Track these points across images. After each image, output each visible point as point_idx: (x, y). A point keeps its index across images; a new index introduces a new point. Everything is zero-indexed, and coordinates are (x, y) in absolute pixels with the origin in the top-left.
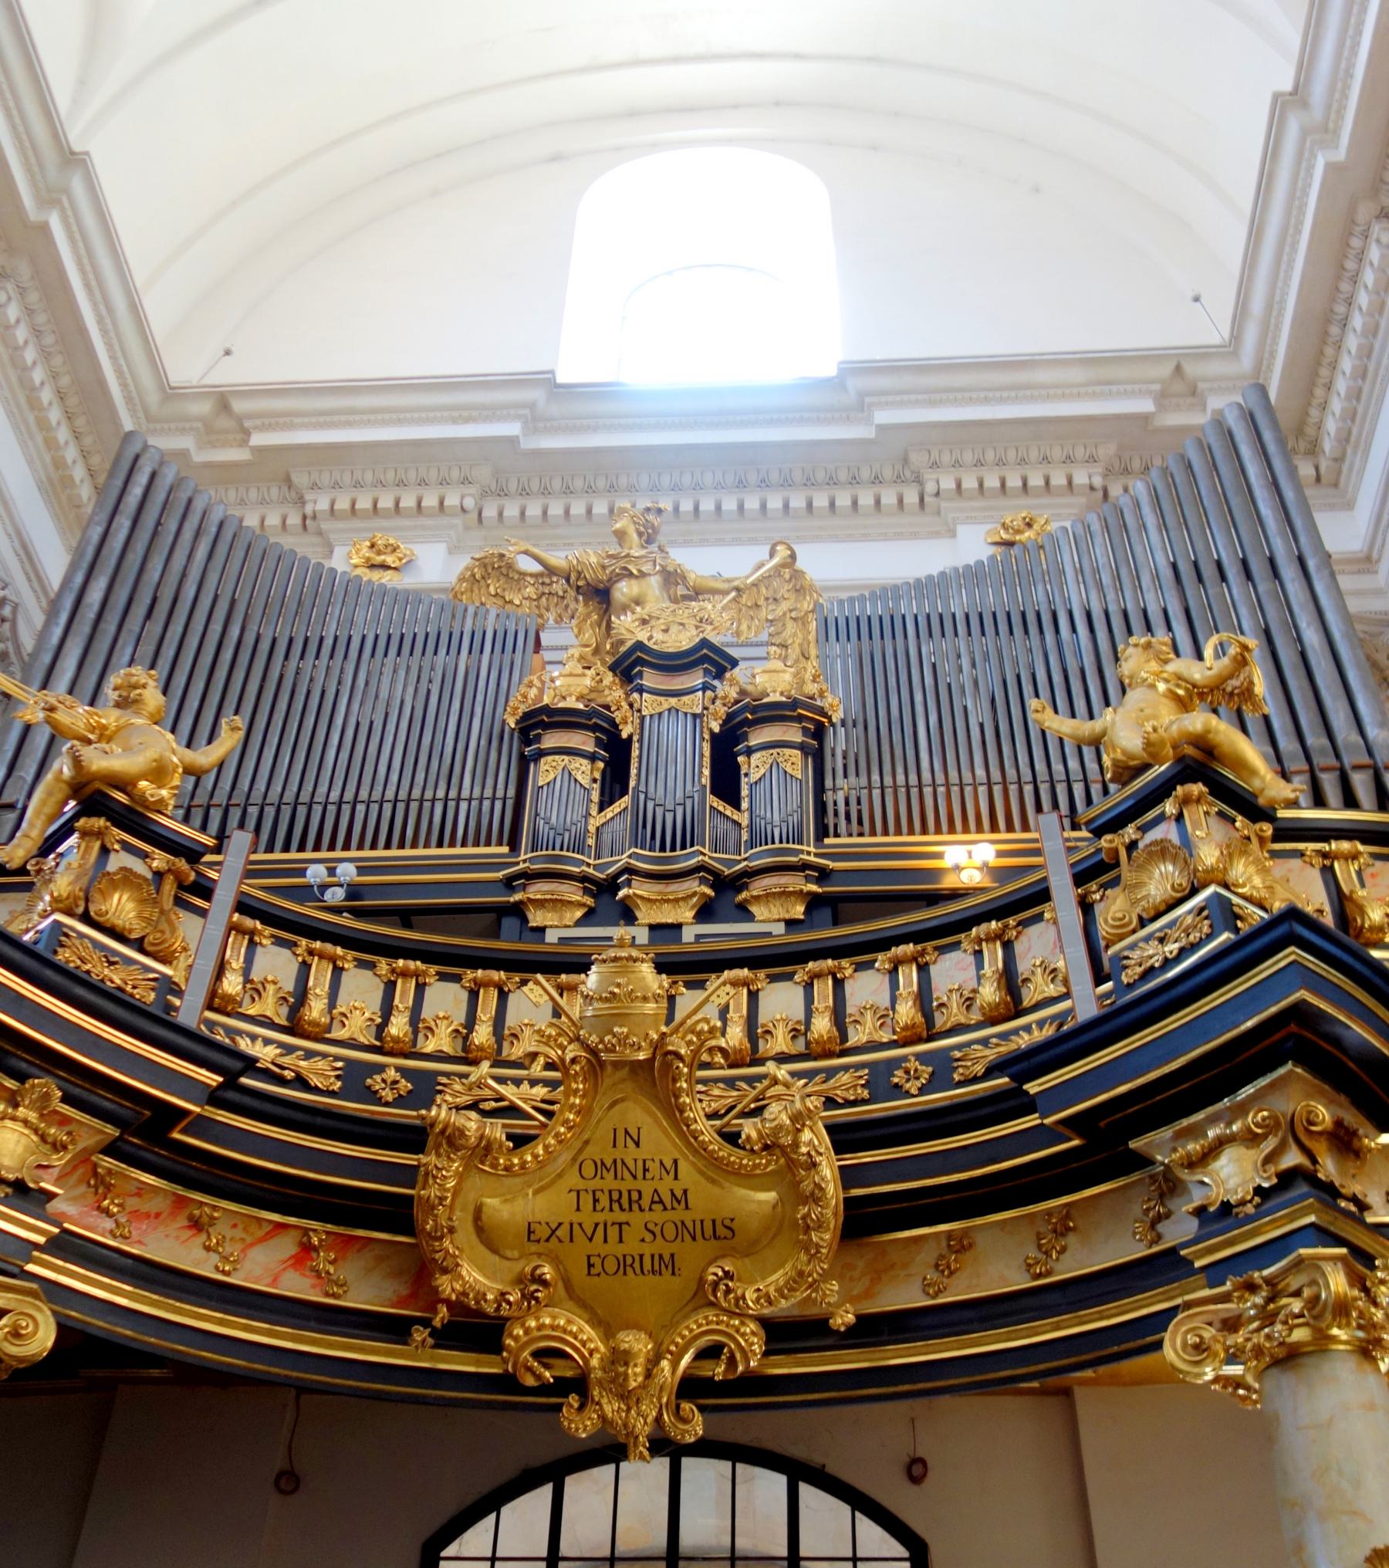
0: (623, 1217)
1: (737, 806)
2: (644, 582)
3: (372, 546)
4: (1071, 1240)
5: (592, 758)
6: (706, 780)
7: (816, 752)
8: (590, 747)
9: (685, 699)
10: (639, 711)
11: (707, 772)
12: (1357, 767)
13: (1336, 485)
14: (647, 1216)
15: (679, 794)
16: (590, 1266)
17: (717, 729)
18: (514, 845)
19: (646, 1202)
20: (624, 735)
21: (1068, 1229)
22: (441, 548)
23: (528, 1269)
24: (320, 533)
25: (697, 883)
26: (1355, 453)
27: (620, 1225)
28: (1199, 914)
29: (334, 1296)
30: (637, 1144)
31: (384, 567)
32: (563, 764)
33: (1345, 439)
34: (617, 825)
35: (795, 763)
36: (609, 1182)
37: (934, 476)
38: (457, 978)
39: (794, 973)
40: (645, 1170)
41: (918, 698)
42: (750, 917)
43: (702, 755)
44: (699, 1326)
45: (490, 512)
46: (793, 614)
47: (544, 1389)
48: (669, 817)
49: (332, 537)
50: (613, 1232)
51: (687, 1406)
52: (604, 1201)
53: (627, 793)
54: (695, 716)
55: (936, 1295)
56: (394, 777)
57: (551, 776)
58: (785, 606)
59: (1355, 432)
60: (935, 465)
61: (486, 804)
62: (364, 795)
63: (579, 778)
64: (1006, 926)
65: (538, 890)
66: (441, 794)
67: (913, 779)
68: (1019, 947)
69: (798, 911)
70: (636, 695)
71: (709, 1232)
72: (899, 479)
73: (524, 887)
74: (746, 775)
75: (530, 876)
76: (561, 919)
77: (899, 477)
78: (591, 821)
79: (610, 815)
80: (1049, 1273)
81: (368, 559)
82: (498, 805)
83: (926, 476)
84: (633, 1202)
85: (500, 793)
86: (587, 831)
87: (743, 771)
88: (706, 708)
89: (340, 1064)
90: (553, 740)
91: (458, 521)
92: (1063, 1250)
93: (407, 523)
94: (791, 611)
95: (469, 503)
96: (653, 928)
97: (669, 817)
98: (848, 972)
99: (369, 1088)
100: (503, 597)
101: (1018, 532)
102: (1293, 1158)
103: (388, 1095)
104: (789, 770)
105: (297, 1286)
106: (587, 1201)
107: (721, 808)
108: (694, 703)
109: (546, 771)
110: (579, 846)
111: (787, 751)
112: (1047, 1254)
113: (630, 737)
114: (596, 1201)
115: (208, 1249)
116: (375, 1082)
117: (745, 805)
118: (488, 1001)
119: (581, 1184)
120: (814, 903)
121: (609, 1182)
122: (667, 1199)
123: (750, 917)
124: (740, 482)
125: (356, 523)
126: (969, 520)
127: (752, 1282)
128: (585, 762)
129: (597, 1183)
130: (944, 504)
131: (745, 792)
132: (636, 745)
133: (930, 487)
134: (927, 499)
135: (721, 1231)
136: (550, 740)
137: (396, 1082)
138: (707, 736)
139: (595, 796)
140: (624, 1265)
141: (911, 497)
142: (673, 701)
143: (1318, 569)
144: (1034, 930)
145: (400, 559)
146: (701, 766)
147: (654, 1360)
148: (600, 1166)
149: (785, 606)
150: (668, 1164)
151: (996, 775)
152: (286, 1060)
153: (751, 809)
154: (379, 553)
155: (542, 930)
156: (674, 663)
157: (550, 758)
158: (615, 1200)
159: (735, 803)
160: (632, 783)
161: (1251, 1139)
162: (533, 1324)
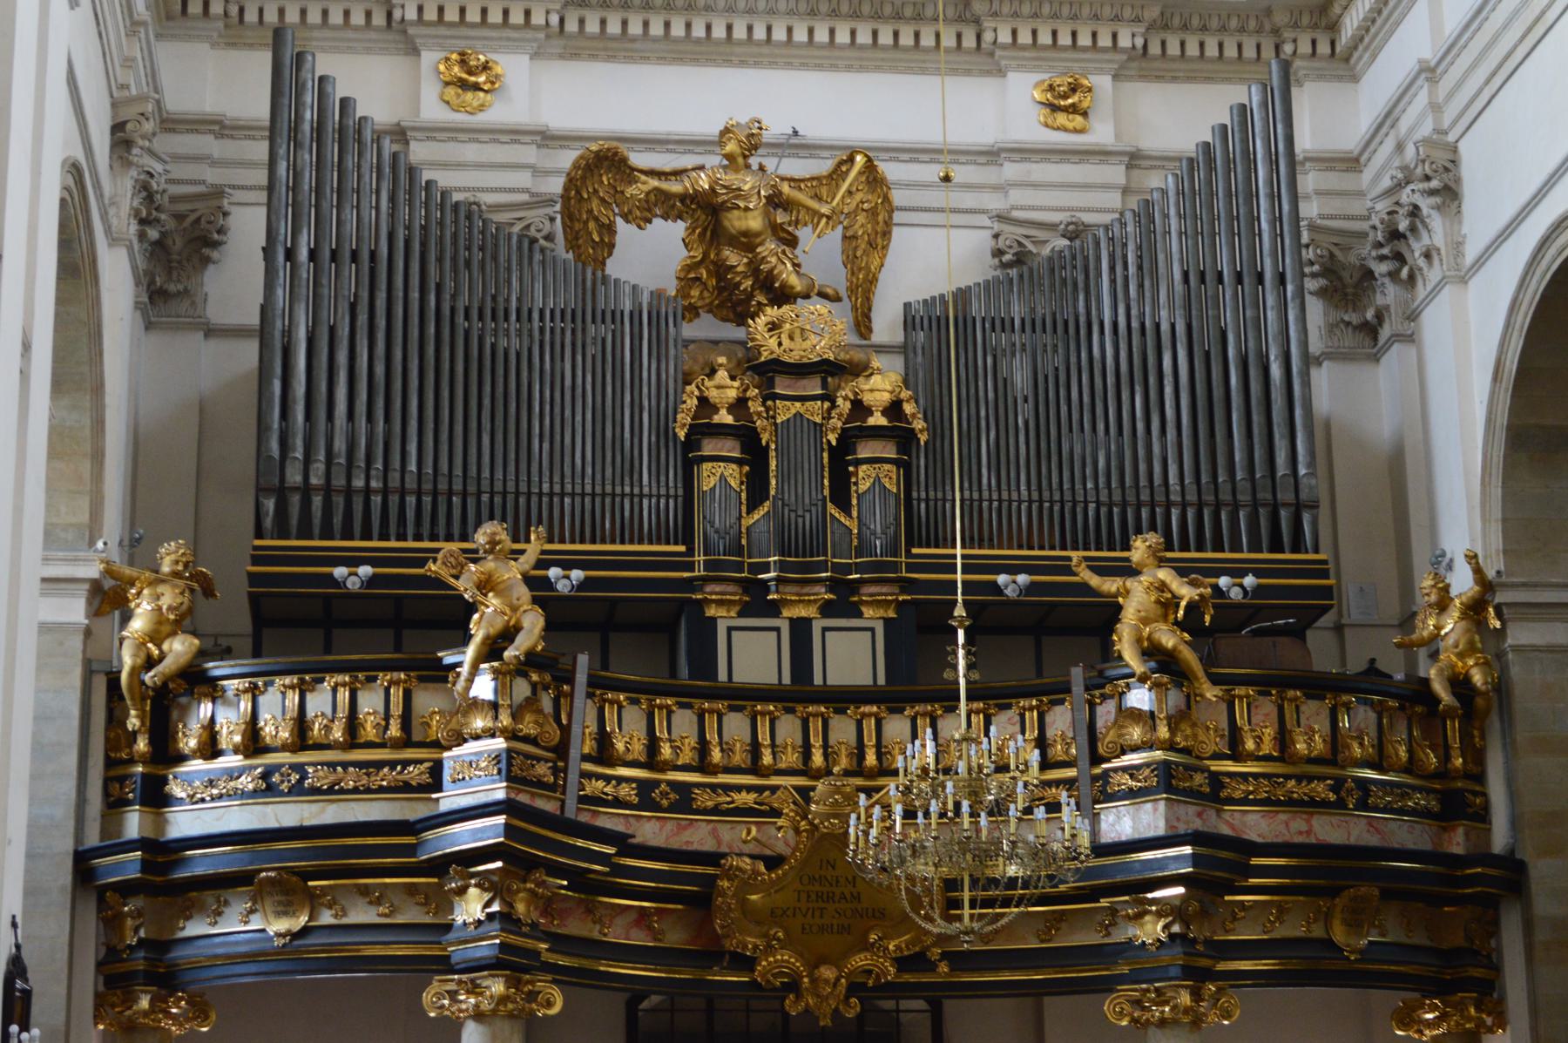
0: (824, 905)
1: (848, 514)
2: (750, 214)
3: (463, 62)
4: (1063, 925)
5: (739, 462)
6: (826, 492)
7: (904, 466)
8: (736, 454)
9: (808, 404)
10: (774, 417)
11: (826, 482)
12: (1285, 505)
13: (1347, 60)
14: (837, 905)
15: (807, 501)
16: (803, 929)
17: (834, 443)
18: (690, 552)
19: (836, 899)
20: (764, 443)
21: (1062, 920)
22: (527, 57)
23: (772, 932)
24: (405, 32)
25: (823, 590)
26: (1366, 48)
27: (822, 909)
28: (1152, 771)
29: (660, 940)
30: (833, 868)
31: (476, 87)
32: (720, 471)
33: (1358, 40)
34: (763, 527)
35: (890, 478)
36: (817, 888)
37: (993, 25)
38: (689, 706)
39: (904, 709)
40: (837, 882)
41: (983, 413)
42: (860, 615)
43: (823, 467)
44: (860, 961)
45: (572, 26)
46: (866, 206)
47: (775, 989)
48: (800, 520)
49: (418, 41)
50: (817, 913)
51: (853, 1000)
52: (813, 897)
53: (768, 498)
54: (815, 424)
55: (987, 943)
56: (589, 471)
57: (712, 485)
58: (859, 197)
59: (1367, 40)
60: (995, 14)
61: (663, 501)
62: (568, 488)
63: (733, 484)
64: (1041, 701)
65: (713, 591)
66: (627, 490)
67: (976, 496)
68: (1048, 719)
69: (891, 614)
70: (769, 403)
71: (870, 914)
72: (960, 19)
73: (701, 590)
74: (856, 484)
75: (705, 580)
76: (728, 611)
77: (960, 17)
78: (743, 522)
79: (756, 517)
80: (1049, 941)
81: (461, 80)
82: (671, 502)
83: (986, 24)
84: (830, 898)
85: (672, 492)
86: (740, 532)
87: (853, 480)
88: (823, 418)
89: (634, 785)
90: (710, 446)
91: (541, 35)
92: (1057, 930)
93: (494, 34)
94: (863, 203)
95: (554, 19)
96: (791, 619)
97: (800, 520)
98: (939, 712)
99: (654, 799)
100: (615, 188)
101: (1065, 97)
102: (1176, 929)
103: (665, 803)
104: (887, 485)
105: (639, 939)
106: (804, 896)
107: (837, 515)
108: (815, 411)
109: (709, 477)
110: (739, 551)
111: (887, 467)
112: (1050, 930)
113: (768, 443)
114: (809, 896)
115: (595, 923)
116: (656, 794)
117: (855, 514)
118: (711, 722)
119: (801, 888)
120: (900, 606)
121: (817, 888)
122: (848, 897)
123: (860, 615)
124: (812, 10)
125: (442, 31)
126: (1020, 68)
127: (893, 939)
128: (734, 466)
129: (810, 888)
130: (998, 53)
131: (854, 502)
132: (772, 454)
133: (988, 37)
134: (983, 45)
135: (877, 914)
136: (709, 447)
137: (667, 794)
138: (825, 446)
139: (744, 495)
140: (822, 929)
141: (969, 42)
142: (798, 404)
143: (1293, 299)
144: (1058, 709)
145: (493, 83)
146: (823, 477)
147: (838, 979)
148: (812, 879)
149: (859, 197)
150: (850, 878)
151: (1035, 496)
152: (608, 789)
153: (858, 517)
154: (470, 73)
155: (714, 620)
156: (800, 370)
157: (710, 464)
158: (819, 896)
159: (846, 508)
160: (772, 492)
161: (1159, 915)
162: (771, 959)
